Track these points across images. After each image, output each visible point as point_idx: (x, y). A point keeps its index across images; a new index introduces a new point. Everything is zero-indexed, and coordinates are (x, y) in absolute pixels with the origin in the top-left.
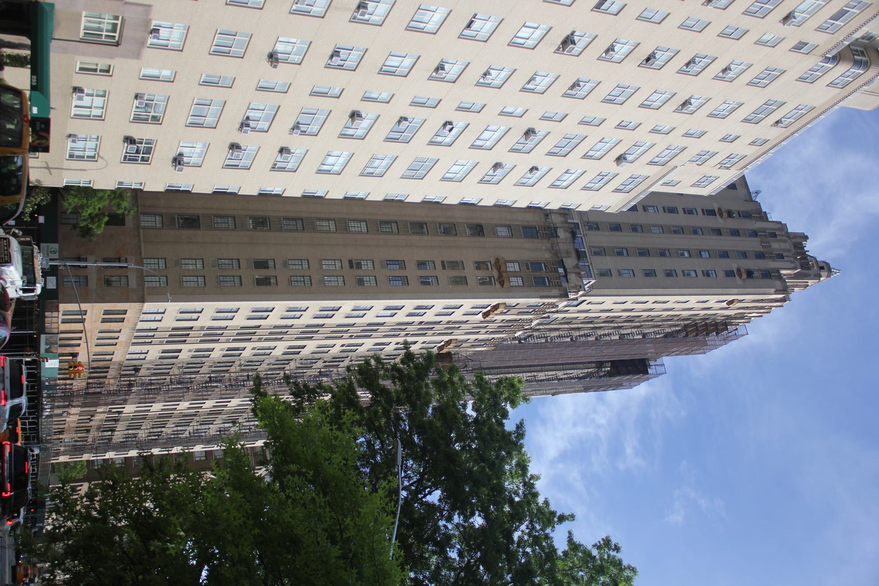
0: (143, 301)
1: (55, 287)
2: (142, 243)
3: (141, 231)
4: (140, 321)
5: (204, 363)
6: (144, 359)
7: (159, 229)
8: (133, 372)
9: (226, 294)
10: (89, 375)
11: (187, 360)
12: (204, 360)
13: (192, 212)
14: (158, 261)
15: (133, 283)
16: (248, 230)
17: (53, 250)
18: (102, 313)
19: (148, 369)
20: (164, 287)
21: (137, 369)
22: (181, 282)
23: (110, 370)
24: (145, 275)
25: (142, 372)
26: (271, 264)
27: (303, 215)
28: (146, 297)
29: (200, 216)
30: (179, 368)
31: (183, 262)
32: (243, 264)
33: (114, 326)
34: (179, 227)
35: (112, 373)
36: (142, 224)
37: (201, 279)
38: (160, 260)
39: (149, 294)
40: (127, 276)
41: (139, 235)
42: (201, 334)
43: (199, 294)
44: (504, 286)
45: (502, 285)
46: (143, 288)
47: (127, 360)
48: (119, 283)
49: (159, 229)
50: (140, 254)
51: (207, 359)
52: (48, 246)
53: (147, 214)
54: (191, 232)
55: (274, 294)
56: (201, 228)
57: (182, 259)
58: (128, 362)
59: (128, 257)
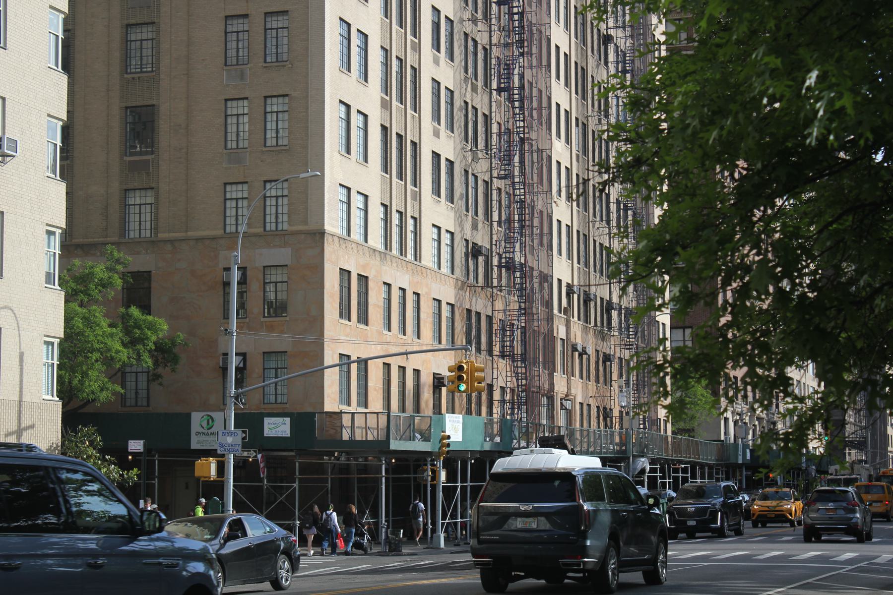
0: (322, 233)
1: (288, 420)
2: (190, 234)
3: (161, 236)
4: (366, 241)
5: (466, 103)
6: (452, 234)
7: (157, 197)
8: (481, 259)
9: (307, 49)
10: (484, 353)
11: (458, 141)
12: (458, 103)
13: (116, 124)
15: (281, 255)
17: (205, 424)
18: (347, 322)
19: (475, 227)
20: (289, 188)
21: (475, 252)
22: (279, 150)
23: (473, 309)
24: (262, 229)
25: (482, 239)
28: (312, 226)
29: (124, 105)
30: (475, 159)
31: (232, 145)
33: (376, 297)
34: (152, 153)
35: (480, 305)
37: (274, 105)
38: (228, 196)
39: (306, 222)
40: (264, 267)
41: (171, 241)
42: (398, 108)
47: (453, 272)
49: (157, 197)
50: (214, 238)
51: (456, 95)
52: (198, 433)
54: (163, 126)
56: (154, 102)
57: (226, 148)
58: (457, 271)
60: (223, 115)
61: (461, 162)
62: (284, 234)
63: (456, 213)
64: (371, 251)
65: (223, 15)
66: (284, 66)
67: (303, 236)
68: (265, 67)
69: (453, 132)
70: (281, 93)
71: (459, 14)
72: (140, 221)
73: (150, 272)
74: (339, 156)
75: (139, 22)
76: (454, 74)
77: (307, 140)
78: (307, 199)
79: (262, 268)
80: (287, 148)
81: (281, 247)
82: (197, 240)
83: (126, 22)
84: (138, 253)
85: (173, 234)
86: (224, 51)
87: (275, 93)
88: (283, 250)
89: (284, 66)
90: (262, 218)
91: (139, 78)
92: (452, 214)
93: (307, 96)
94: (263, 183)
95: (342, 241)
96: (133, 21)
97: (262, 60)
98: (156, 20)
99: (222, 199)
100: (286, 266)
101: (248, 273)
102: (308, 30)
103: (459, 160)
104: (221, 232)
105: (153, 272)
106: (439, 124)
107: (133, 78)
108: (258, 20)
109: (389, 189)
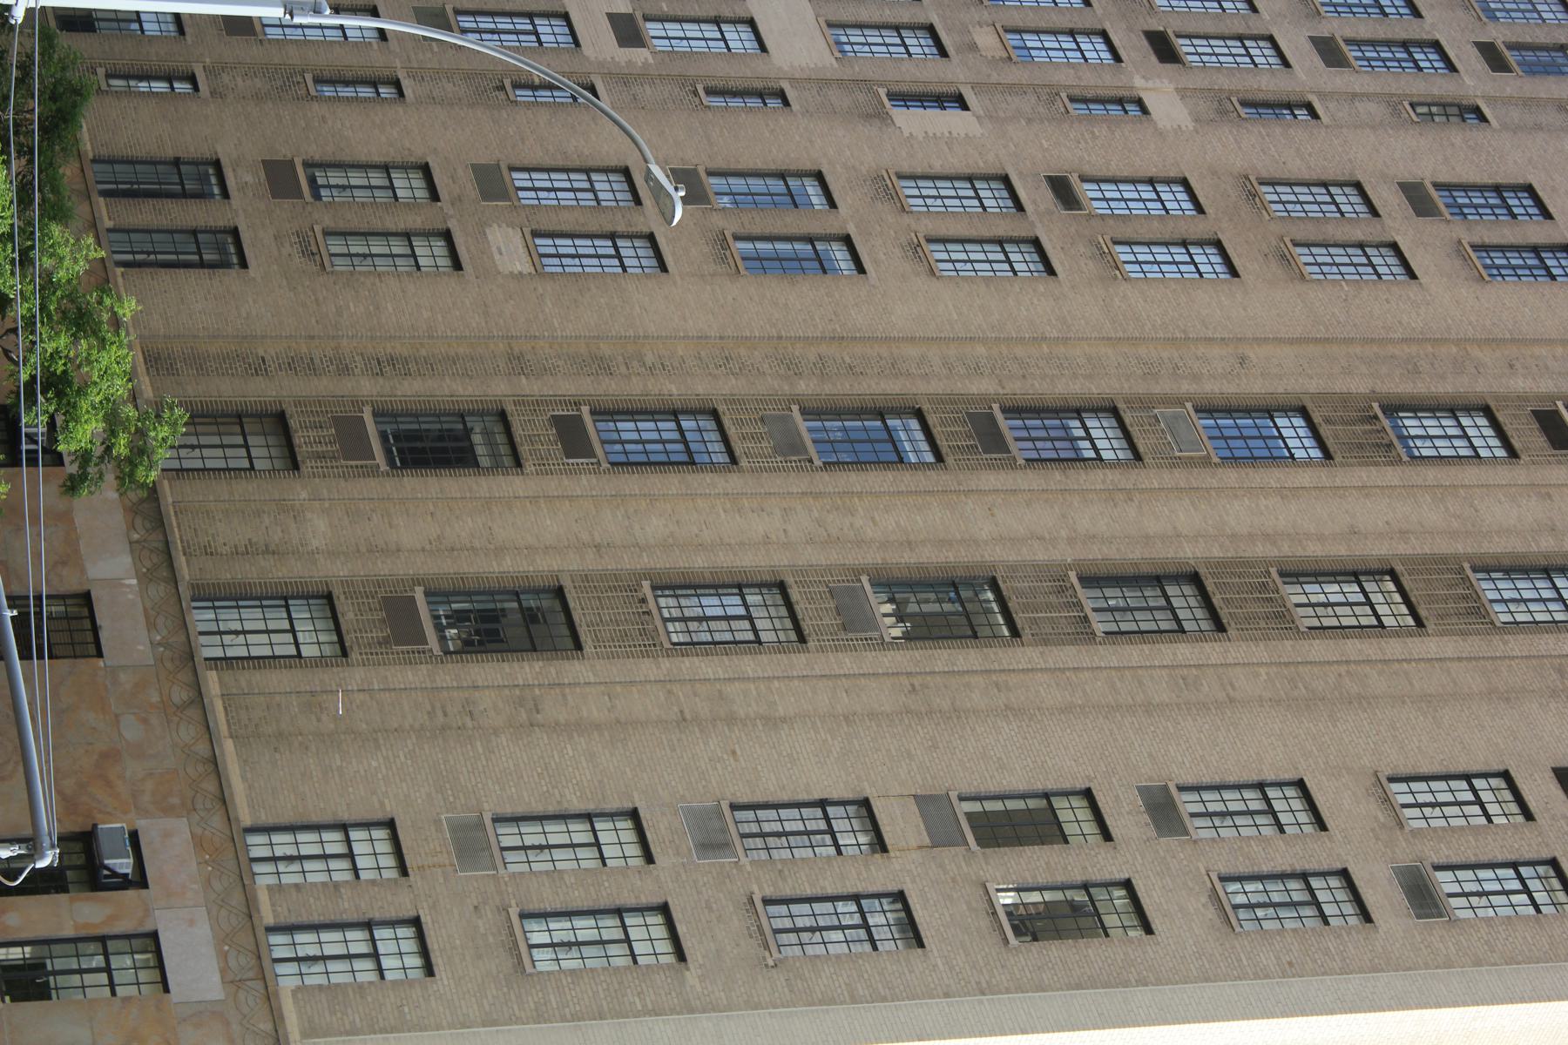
2: (229, 745)
3: (212, 682)
7: (320, 662)
9: (832, 1001)
13: (509, 566)
14: (348, 841)
16: (883, 645)
20: (407, 982)
22: (517, 953)
24: (269, 920)
26: (1073, 815)
27: (1190, 553)
31: (509, 836)
32: (901, 824)
34: (447, 652)
36: (209, 649)
37: (647, 934)
38: (355, 835)
40: (154, 936)
41: (198, 696)
43: (656, 1012)
46: (270, 998)
48: (103, 978)
49: (320, 662)
50: (223, 800)
53: (238, 596)
54: (527, 670)
55: (1143, 982)
57: (498, 820)
59: (141, 824)
60: (590, 807)
62: (262, 970)
65: (869, 792)
66: (767, 947)
67: (267, 1026)
68: (751, 901)
70: (687, 944)
72: (244, 632)
73: (100, 654)
75: (797, 608)
77: (563, 1019)
78: (383, 1031)
79: (148, 928)
80: (529, 969)
81: (223, 972)
82: (214, 763)
83: (790, 580)
84: (151, 626)
85: (219, 706)
86: (771, 799)
87: (681, 929)
88: (217, 978)
89: (767, 947)
90: (304, 919)
91: (649, 613)
93: (692, 1011)
94: (412, 914)
96: (795, 594)
97: (769, 892)
98: (811, 644)
99: (345, 817)
100: (166, 990)
101: (131, 894)
102: (884, 999)
104: (247, 820)
105: (101, 663)
107: (643, 601)
108: (879, 875)
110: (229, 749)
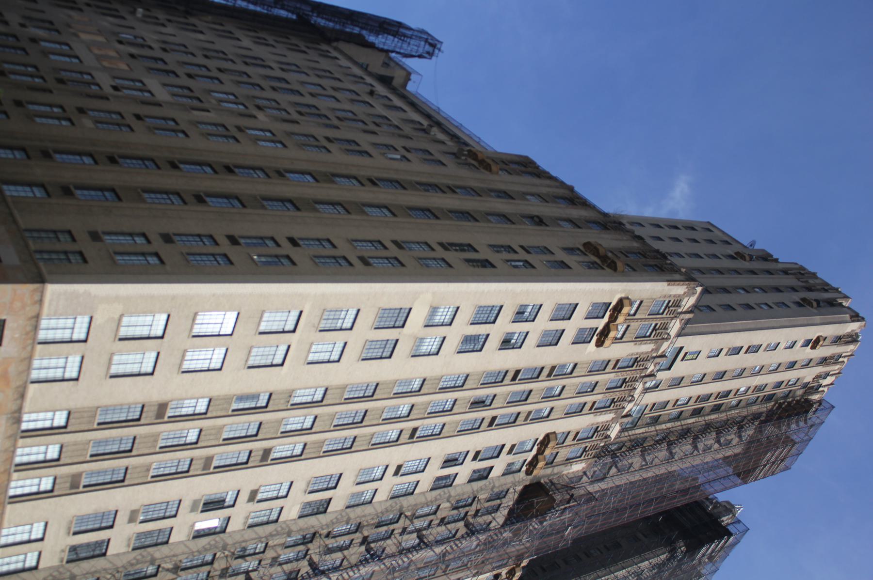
0: (41, 279)
4: (33, 382)
12: (159, 553)
22: (114, 262)
44: (618, 269)
45: (615, 269)
50: (15, 222)
51: (164, 549)
61: (105, 570)
63: (56, 569)
64: (21, 389)
69: (134, 549)
71: (230, 541)
74: (117, 316)
76: (182, 542)
82: (11, 215)
92: (55, 562)
95: (35, 319)
103: (109, 565)
106: (142, 522)
109: (83, 428)
110: (16, 213)
